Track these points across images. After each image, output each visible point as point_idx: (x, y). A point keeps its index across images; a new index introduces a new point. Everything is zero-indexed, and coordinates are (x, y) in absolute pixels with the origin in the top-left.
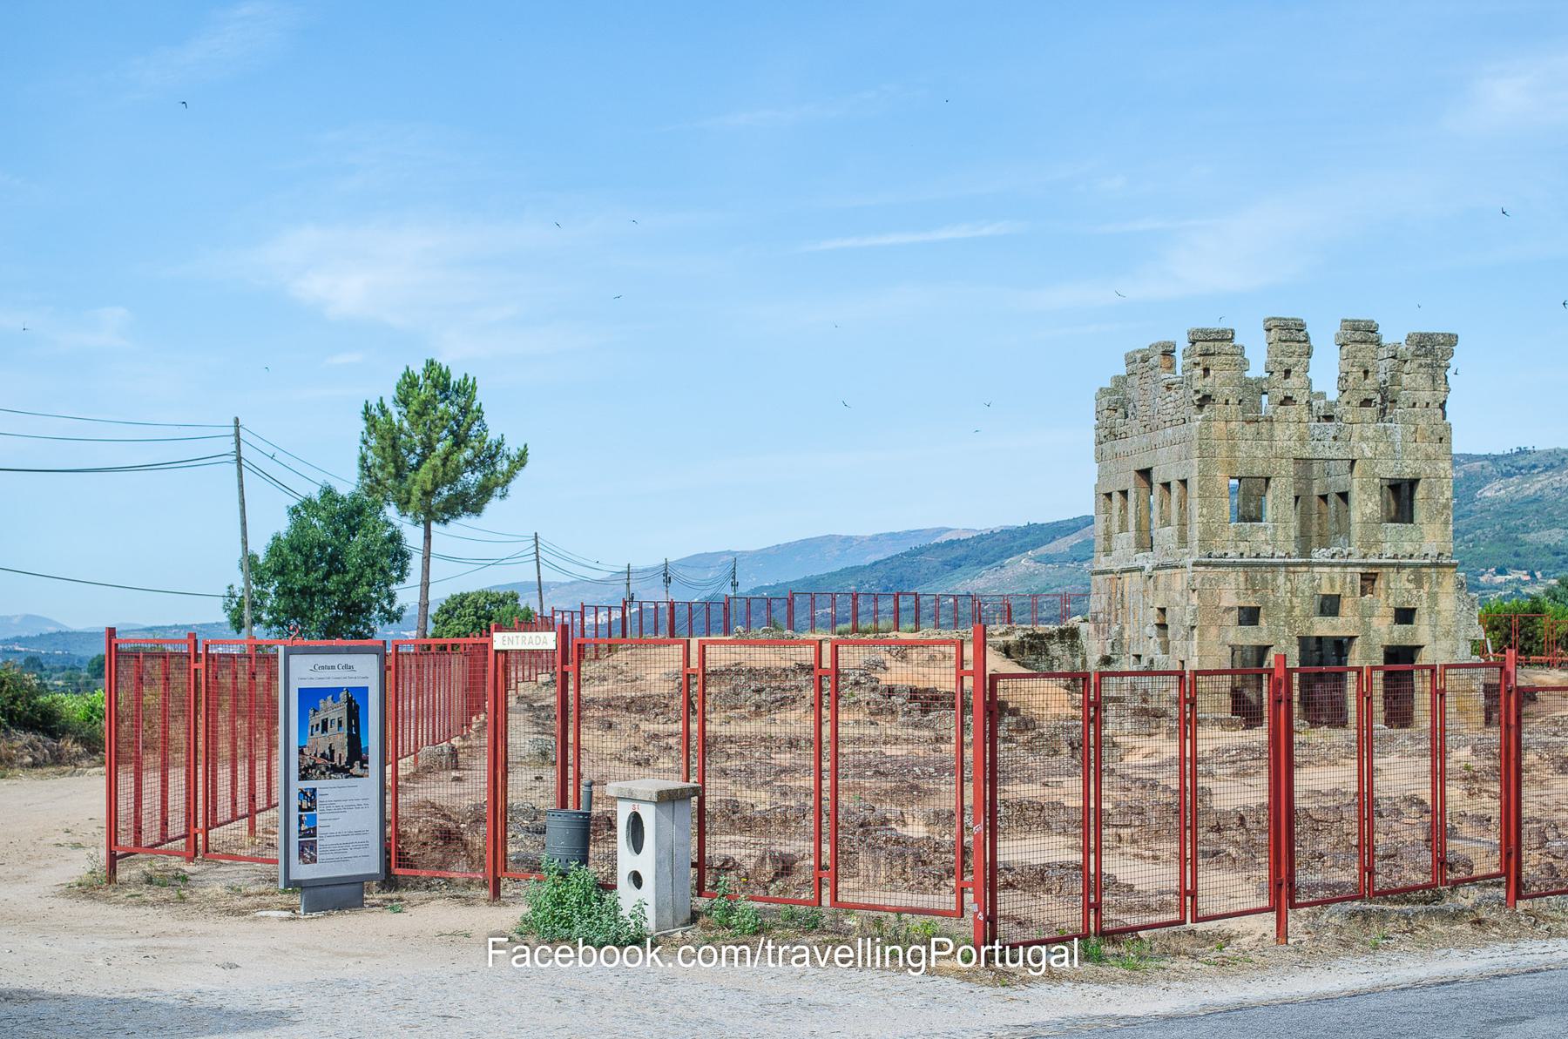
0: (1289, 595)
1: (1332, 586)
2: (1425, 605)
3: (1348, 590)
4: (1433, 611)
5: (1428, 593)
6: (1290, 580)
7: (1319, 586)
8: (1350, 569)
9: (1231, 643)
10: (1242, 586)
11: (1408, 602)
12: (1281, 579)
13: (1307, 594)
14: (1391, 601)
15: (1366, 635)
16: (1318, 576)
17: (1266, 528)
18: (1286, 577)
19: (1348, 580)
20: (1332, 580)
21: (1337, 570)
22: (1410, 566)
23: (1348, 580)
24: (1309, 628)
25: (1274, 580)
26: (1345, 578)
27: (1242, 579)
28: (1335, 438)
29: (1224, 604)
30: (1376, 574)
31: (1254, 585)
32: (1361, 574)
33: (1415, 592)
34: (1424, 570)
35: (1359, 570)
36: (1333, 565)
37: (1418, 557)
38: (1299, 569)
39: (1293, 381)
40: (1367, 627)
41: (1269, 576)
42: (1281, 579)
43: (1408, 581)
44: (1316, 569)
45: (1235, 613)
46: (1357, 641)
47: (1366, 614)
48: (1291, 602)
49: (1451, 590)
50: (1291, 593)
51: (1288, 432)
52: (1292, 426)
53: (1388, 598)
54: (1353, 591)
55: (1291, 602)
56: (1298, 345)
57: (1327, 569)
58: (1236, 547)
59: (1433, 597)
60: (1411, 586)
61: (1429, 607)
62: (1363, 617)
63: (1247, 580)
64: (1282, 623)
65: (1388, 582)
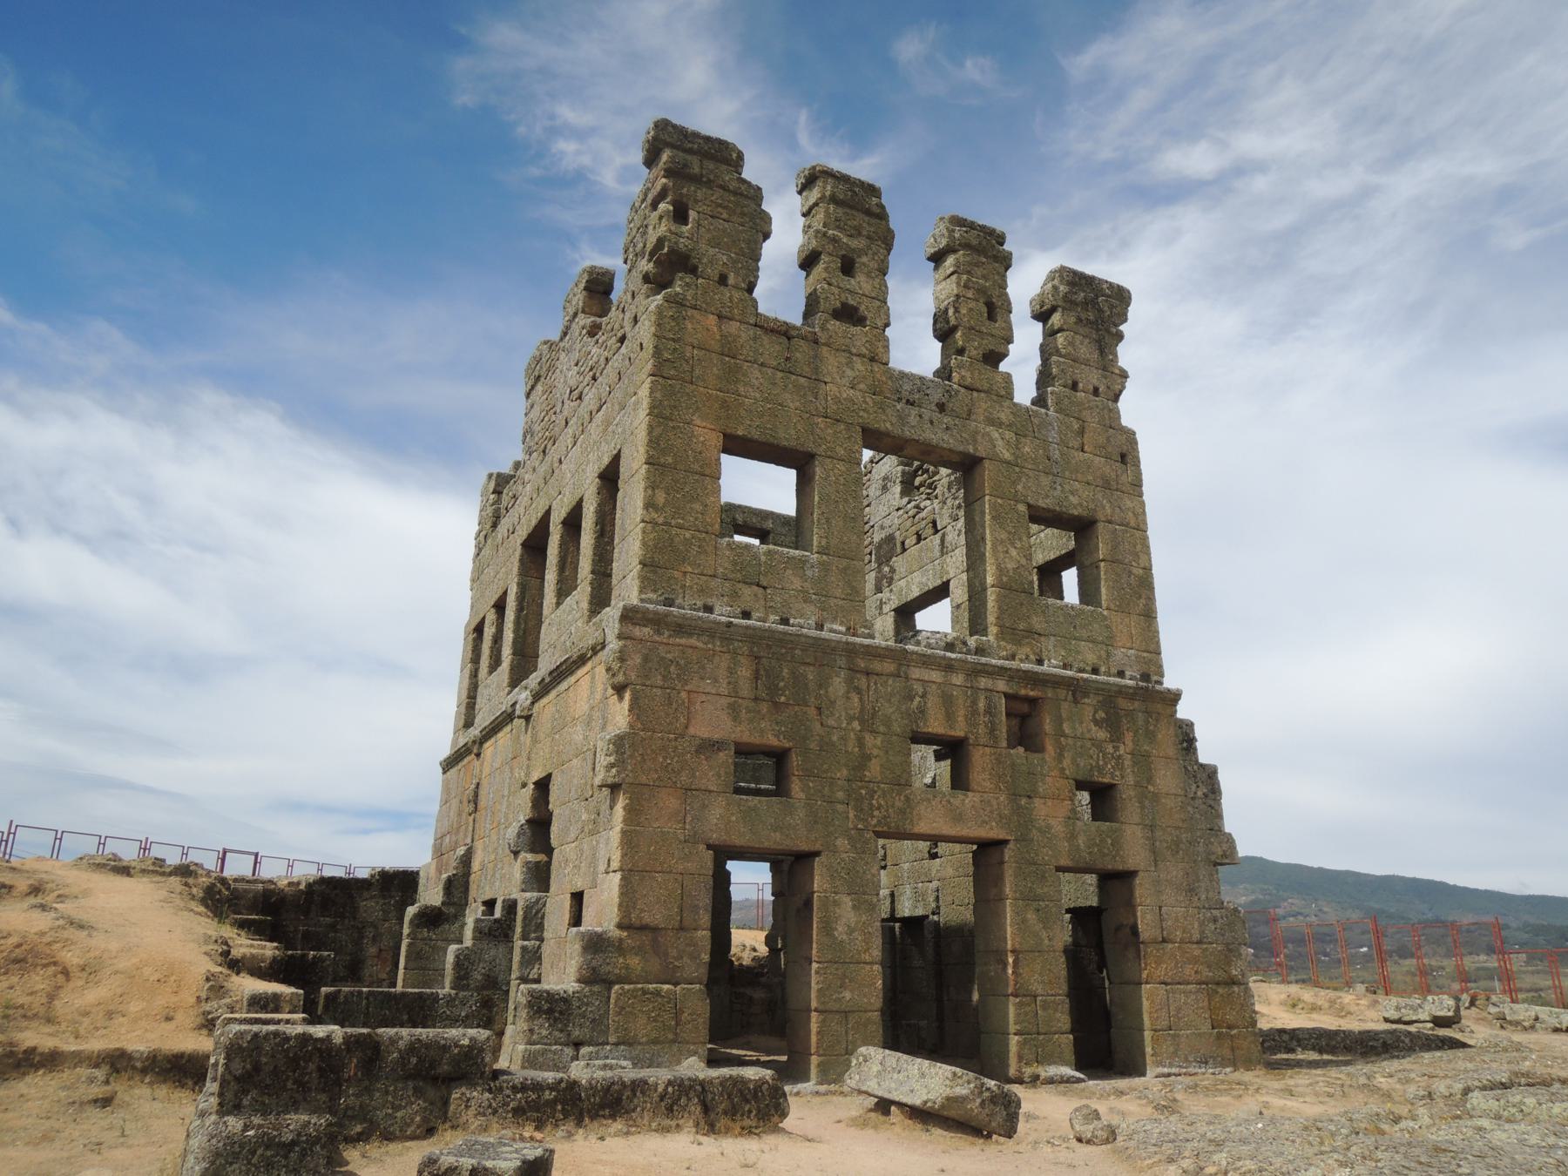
0: (856, 725)
1: (950, 717)
2: (1131, 780)
3: (982, 730)
4: (1149, 798)
5: (1132, 754)
6: (858, 691)
7: (922, 711)
8: (983, 682)
9: (715, 837)
10: (745, 689)
11: (1100, 770)
12: (838, 685)
13: (896, 728)
14: (1066, 762)
15: (1023, 839)
16: (919, 688)
17: (803, 562)
18: (849, 681)
19: (981, 705)
20: (947, 701)
21: (958, 679)
22: (1101, 689)
23: (981, 705)
24: (902, 812)
25: (823, 683)
26: (974, 703)
27: (745, 672)
28: (941, 407)
29: (701, 729)
31: (773, 690)
32: (1007, 695)
33: (1110, 749)
34: (1123, 703)
35: (1001, 685)
36: (949, 667)
37: (1105, 674)
38: (877, 666)
39: (861, 283)
40: (1022, 820)
41: (811, 674)
42: (838, 685)
43: (1096, 722)
44: (916, 673)
45: (725, 757)
46: (1008, 853)
47: (1021, 791)
48: (861, 743)
49: (1171, 752)
50: (862, 722)
51: (849, 372)
52: (859, 365)
53: (1060, 757)
54: (992, 731)
55: (861, 743)
56: (866, 219)
57: (936, 676)
58: (735, 595)
59: (1143, 761)
60: (1102, 734)
61: (1137, 785)
62: (1014, 796)
63: (757, 676)
64: (840, 795)
65: (1059, 721)
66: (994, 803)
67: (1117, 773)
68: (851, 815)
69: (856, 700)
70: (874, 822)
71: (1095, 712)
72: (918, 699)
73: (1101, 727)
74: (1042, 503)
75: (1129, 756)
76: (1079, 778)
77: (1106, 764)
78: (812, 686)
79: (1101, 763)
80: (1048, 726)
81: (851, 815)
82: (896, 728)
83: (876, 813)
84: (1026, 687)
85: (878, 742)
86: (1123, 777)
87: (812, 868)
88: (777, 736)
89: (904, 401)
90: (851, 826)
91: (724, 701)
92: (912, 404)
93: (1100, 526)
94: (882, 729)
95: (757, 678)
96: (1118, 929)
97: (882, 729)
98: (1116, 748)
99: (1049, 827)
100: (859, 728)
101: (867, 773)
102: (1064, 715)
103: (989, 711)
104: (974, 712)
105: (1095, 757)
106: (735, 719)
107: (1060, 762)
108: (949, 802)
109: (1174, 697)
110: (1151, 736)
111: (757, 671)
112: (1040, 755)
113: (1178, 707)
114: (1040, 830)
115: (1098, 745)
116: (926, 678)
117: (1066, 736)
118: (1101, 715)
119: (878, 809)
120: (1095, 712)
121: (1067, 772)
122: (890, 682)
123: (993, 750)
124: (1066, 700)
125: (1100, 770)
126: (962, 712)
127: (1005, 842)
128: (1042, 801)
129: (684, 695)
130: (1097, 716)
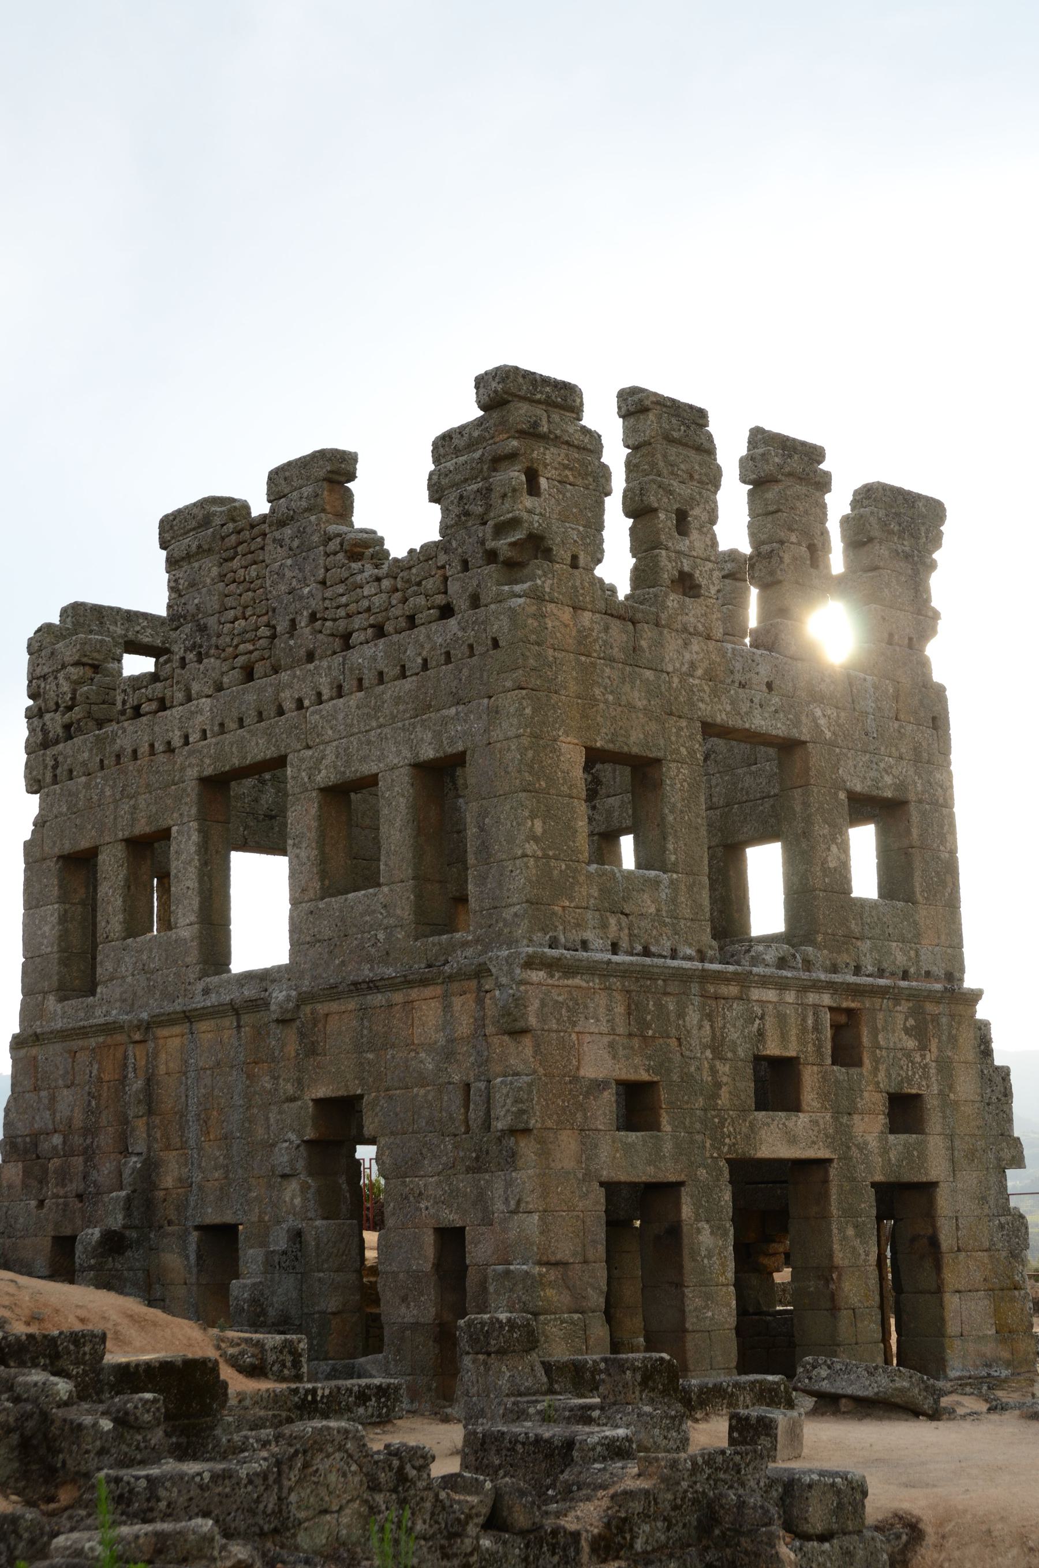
0: (708, 1053)
2: (935, 1088)
3: (810, 1048)
4: (948, 1105)
7: (761, 1034)
13: (741, 1053)
15: (846, 1158)
22: (913, 996)
26: (804, 1020)
30: (850, 1012)
32: (831, 1009)
33: (918, 1059)
38: (724, 990)
43: (907, 1031)
44: (756, 994)
50: (714, 1050)
54: (819, 1048)
61: (941, 1093)
62: (837, 1114)
66: (821, 1122)
67: (924, 1083)
68: (708, 1145)
69: (708, 1028)
70: (726, 1149)
71: (906, 1019)
72: (758, 1021)
73: (910, 1036)
74: (858, 788)
75: (934, 1064)
76: (892, 1091)
77: (914, 1074)
78: (673, 1017)
79: (910, 1073)
80: (866, 1040)
81: (708, 1145)
82: (741, 1053)
83: (727, 1140)
84: (847, 1000)
85: (727, 1069)
86: (928, 1087)
87: (679, 1197)
88: (648, 1071)
89: (737, 684)
90: (708, 1155)
91: (606, 1040)
92: (744, 687)
93: (913, 808)
94: (730, 1055)
95: (629, 1014)
96: (914, 1239)
97: (730, 1055)
98: (923, 1057)
99: (866, 1143)
100: (711, 1056)
101: (719, 1102)
102: (880, 1026)
103: (817, 1028)
104: (804, 1030)
105: (905, 1067)
106: (614, 1058)
107: (876, 1076)
108: (784, 1124)
109: (976, 996)
110: (953, 1040)
111: (629, 1006)
112: (858, 1070)
113: (978, 1007)
114: (858, 1146)
115: (908, 1055)
116: (764, 999)
117: (881, 1048)
118: (911, 1022)
119: (729, 1137)
120: (906, 1019)
121: (881, 1085)
122: (735, 1006)
123: (820, 1068)
124: (881, 1010)
125: (909, 1080)
126: (794, 1032)
127: (830, 1161)
128: (860, 1117)
129: (574, 1036)
130: (908, 1025)
